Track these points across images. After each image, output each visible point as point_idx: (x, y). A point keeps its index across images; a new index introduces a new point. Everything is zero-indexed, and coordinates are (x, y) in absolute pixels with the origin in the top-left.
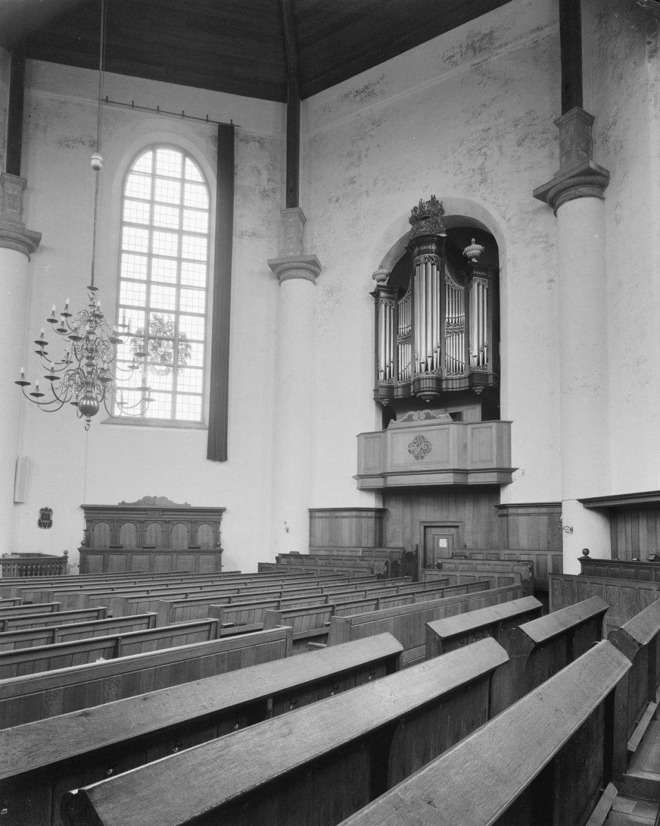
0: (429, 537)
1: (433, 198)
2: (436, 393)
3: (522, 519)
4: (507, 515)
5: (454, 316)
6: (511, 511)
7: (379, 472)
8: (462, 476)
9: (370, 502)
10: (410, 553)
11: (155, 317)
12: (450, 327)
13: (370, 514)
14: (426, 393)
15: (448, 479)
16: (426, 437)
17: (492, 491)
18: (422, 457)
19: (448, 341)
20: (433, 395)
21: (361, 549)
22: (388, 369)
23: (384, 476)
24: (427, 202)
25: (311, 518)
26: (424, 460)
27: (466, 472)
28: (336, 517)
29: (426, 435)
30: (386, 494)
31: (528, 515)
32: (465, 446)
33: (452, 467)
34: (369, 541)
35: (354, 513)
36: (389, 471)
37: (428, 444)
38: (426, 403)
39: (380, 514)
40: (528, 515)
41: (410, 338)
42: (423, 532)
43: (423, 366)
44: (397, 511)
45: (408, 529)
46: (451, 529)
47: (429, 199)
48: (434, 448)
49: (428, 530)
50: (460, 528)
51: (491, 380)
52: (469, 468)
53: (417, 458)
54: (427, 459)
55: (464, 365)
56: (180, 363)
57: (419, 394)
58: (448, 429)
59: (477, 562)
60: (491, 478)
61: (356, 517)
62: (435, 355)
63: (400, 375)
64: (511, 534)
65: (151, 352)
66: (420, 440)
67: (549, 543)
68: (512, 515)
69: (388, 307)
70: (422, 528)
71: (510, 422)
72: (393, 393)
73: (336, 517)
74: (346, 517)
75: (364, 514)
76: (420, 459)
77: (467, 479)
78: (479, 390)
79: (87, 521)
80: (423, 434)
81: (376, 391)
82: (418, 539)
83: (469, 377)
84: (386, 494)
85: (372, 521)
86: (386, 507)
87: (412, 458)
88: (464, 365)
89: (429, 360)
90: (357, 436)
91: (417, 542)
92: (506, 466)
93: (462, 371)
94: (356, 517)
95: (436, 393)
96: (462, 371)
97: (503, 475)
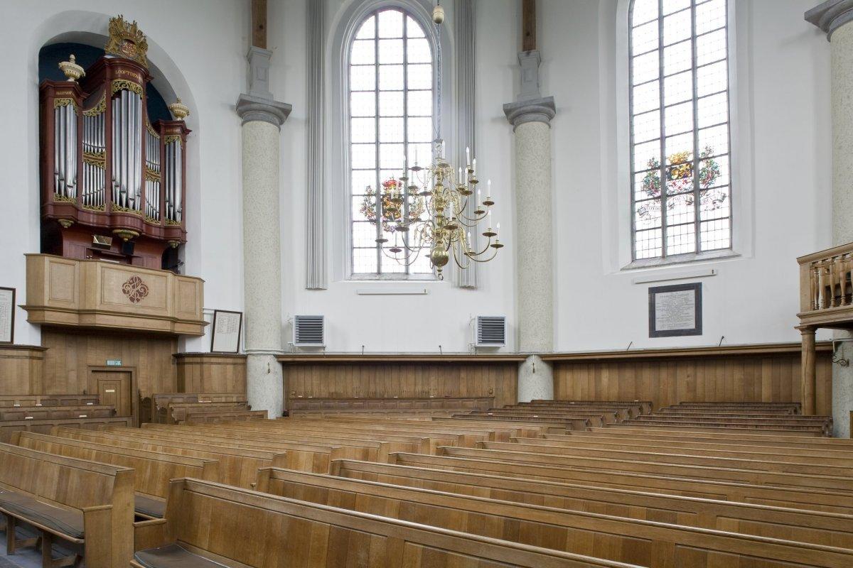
3: (214, 367)
18: (138, 300)
20: (135, 236)
26: (139, 304)
30: (48, 330)
33: (169, 316)
35: (27, 353)
36: (98, 308)
37: (145, 288)
38: (124, 241)
46: (118, 374)
48: (151, 291)
53: (132, 300)
54: (144, 301)
55: (158, 214)
66: (134, 281)
68: (206, 363)
74: (13, 357)
76: (135, 301)
80: (139, 276)
87: (125, 299)
90: (27, 255)
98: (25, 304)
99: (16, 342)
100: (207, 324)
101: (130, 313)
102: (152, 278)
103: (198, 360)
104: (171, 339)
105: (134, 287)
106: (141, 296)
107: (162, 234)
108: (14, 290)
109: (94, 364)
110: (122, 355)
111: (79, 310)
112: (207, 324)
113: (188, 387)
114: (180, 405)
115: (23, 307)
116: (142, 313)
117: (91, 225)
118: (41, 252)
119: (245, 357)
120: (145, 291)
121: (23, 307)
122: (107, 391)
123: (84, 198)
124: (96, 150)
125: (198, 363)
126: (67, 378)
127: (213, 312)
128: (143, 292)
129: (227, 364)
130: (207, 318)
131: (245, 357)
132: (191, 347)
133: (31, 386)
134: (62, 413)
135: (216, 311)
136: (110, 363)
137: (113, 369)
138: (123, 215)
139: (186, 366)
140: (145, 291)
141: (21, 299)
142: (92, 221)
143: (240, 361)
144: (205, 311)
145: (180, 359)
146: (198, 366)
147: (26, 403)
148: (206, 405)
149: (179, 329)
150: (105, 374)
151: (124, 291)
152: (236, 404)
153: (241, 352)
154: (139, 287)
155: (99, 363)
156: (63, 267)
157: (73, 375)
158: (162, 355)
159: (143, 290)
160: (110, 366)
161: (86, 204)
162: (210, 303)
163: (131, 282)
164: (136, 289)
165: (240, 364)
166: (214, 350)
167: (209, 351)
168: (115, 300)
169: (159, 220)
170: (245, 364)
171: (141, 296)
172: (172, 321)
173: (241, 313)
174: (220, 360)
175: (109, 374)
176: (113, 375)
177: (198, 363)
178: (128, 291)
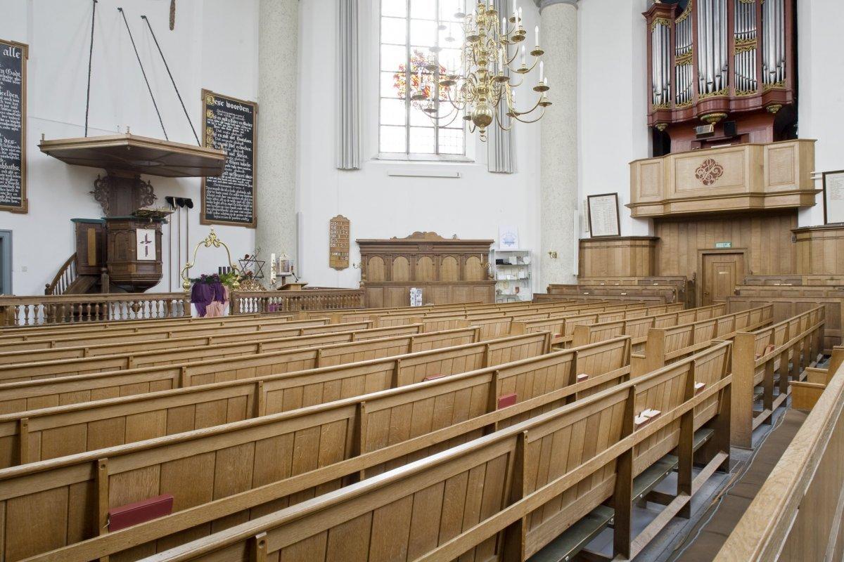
0: (708, 265)
3: (828, 242)
4: (810, 239)
5: (743, 31)
6: (814, 234)
7: (659, 199)
9: (643, 230)
10: (691, 281)
11: (416, 52)
12: (739, 44)
13: (644, 243)
14: (713, 115)
15: (745, 204)
17: (791, 213)
18: (712, 182)
19: (738, 58)
20: (722, 117)
21: (637, 279)
22: (665, 92)
23: (665, 203)
25: (581, 248)
26: (714, 185)
27: (763, 196)
28: (608, 247)
29: (717, 159)
31: (836, 238)
32: (762, 167)
33: (748, 191)
34: (643, 270)
35: (628, 243)
36: (672, 197)
39: (654, 241)
40: (836, 238)
41: (692, 57)
42: (701, 260)
43: (710, 87)
44: (670, 239)
45: (685, 257)
46: (732, 256)
48: (726, 171)
49: (707, 257)
50: (745, 256)
51: (789, 97)
52: (766, 191)
53: (705, 183)
54: (718, 182)
55: (755, 83)
56: (440, 98)
57: (702, 118)
58: (744, 150)
60: (793, 201)
61: (631, 246)
62: (723, 74)
63: (678, 98)
65: (413, 88)
66: (707, 165)
69: (664, 27)
70: (701, 256)
71: (814, 141)
72: (671, 116)
73: (608, 247)
74: (619, 246)
75: (638, 243)
76: (709, 184)
77: (763, 202)
78: (774, 109)
79: (362, 255)
81: (651, 115)
82: (694, 268)
83: (762, 96)
84: (657, 222)
85: (646, 251)
86: (659, 236)
87: (699, 183)
88: (755, 83)
89: (717, 80)
90: (630, 163)
91: (695, 270)
92: (809, 188)
93: (753, 90)
94: (631, 246)
95: (721, 115)
96: (753, 90)
97: (806, 197)
99: (623, 235)
100: (818, 191)
101: (700, 197)
102: (727, 156)
103: (806, 235)
104: (791, 213)
105: (707, 170)
108: (616, 194)
109: (703, 248)
110: (731, 237)
111: (660, 202)
112: (818, 191)
113: (799, 271)
115: (627, 206)
116: (716, 194)
117: (682, 121)
118: (774, 141)
120: (719, 171)
121: (627, 206)
123: (678, 98)
124: (746, 35)
126: (679, 262)
127: (821, 176)
128: (718, 172)
130: (818, 185)
133: (634, 268)
134: (634, 292)
135: (824, 174)
136: (719, 245)
137: (721, 252)
138: (705, 101)
139: (586, 250)
140: (719, 171)
141: (625, 199)
142: (680, 117)
144: (816, 176)
146: (807, 242)
148: (785, 288)
151: (697, 176)
152: (831, 288)
154: (713, 168)
155: (709, 246)
157: (684, 259)
158: (778, 234)
159: (717, 171)
160: (719, 249)
161: (680, 103)
162: (820, 167)
163: (704, 165)
164: (708, 173)
166: (828, 222)
168: (688, 186)
172: (750, 197)
176: (728, 258)
177: (806, 239)
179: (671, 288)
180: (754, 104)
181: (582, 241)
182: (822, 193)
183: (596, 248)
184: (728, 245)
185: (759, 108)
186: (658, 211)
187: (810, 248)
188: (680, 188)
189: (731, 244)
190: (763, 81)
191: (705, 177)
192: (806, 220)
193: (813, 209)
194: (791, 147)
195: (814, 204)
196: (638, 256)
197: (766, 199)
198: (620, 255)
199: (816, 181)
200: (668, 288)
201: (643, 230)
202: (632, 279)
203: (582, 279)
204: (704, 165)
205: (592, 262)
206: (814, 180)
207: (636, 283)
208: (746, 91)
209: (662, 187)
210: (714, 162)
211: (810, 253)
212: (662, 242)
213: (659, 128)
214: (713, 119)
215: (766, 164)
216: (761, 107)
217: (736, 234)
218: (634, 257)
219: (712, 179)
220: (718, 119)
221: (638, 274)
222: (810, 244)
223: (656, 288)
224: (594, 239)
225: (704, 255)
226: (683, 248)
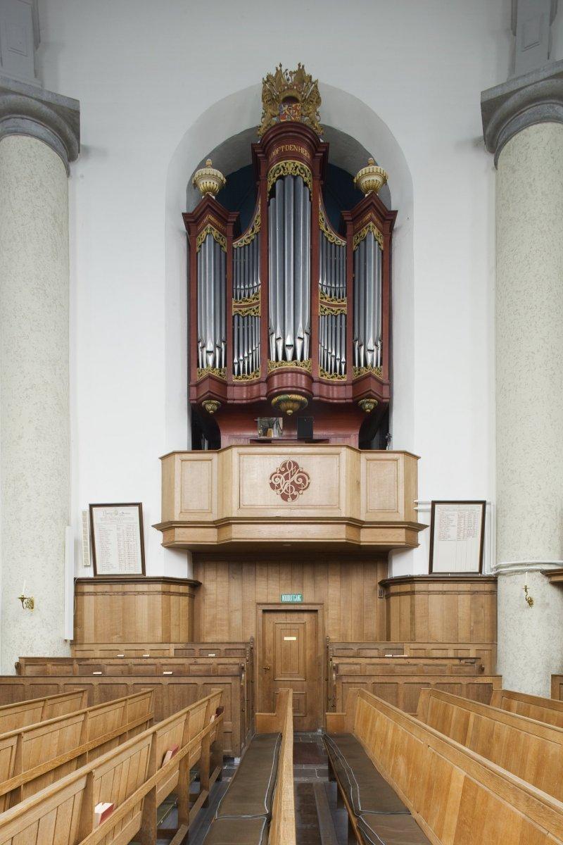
0: (269, 627)
1: (301, 71)
2: (303, 398)
4: (413, 593)
6: (418, 587)
8: (353, 531)
15: (337, 534)
16: (300, 466)
18: (294, 497)
21: (172, 647)
23: (223, 524)
24: (291, 73)
25: (78, 594)
26: (296, 502)
28: (124, 593)
30: (199, 556)
32: (359, 483)
33: (343, 515)
34: (180, 633)
35: (159, 587)
36: (234, 515)
37: (305, 477)
47: (296, 68)
49: (267, 615)
52: (363, 519)
53: (284, 497)
54: (303, 498)
57: (275, 400)
59: (368, 661)
60: (398, 536)
61: (164, 593)
64: (418, 620)
67: (471, 632)
70: (260, 612)
71: (417, 458)
72: (226, 393)
73: (124, 593)
74: (143, 593)
75: (173, 588)
76: (290, 499)
78: (369, 406)
84: (199, 556)
85: (184, 601)
86: (201, 580)
87: (274, 497)
94: (164, 593)
96: (340, 374)
98: (159, 521)
99: (149, 574)
100: (422, 527)
105: (287, 478)
106: (298, 490)
107: (350, 394)
108: (139, 505)
109: (265, 601)
111: (214, 522)
112: (422, 527)
114: (351, 660)
119: (493, 580)
122: (286, 639)
125: (406, 593)
127: (430, 507)
129: (459, 593)
130: (423, 519)
131: (493, 580)
132: (401, 567)
133: (167, 630)
135: (434, 503)
140: (304, 481)
141: (154, 515)
142: (238, 395)
143: (487, 587)
144: (419, 507)
145: (386, 585)
147: (106, 654)
149: (367, 537)
150: (283, 615)
151: (272, 485)
152: (457, 662)
153: (487, 571)
156: (198, 464)
157: (237, 617)
159: (300, 479)
161: (239, 374)
162: (426, 495)
163: (283, 469)
165: (484, 592)
167: (425, 572)
168: (259, 501)
169: (345, 373)
170: (494, 593)
171: (298, 490)
172: (347, 524)
173: (484, 503)
174: (446, 587)
175: (289, 615)
178: (279, 485)
179: (237, 661)
180: (340, 394)
181: (79, 582)
182: (428, 530)
183: (103, 593)
184: (298, 599)
185: (348, 401)
186: (209, 537)
187: (412, 606)
188: (246, 502)
189: (302, 598)
190: (354, 364)
191: (284, 488)
192: (401, 567)
193: (415, 551)
194: (394, 460)
195: (417, 545)
196: (174, 610)
197: (363, 532)
198: (146, 606)
199: (419, 514)
200: (231, 661)
201: (179, 568)
202: (165, 646)
203: (78, 647)
204: (283, 469)
205: (96, 619)
206: (417, 511)
207: (172, 654)
208: (331, 373)
209: (215, 500)
210: (297, 468)
211: (412, 613)
212: (205, 590)
213: (209, 407)
214: (291, 405)
215: (363, 481)
216: (351, 401)
217: (308, 583)
218: (167, 611)
219: (295, 493)
220: (296, 406)
221: (173, 638)
222: (412, 600)
223: (212, 661)
224: (98, 580)
225: (264, 611)
226: (236, 603)
